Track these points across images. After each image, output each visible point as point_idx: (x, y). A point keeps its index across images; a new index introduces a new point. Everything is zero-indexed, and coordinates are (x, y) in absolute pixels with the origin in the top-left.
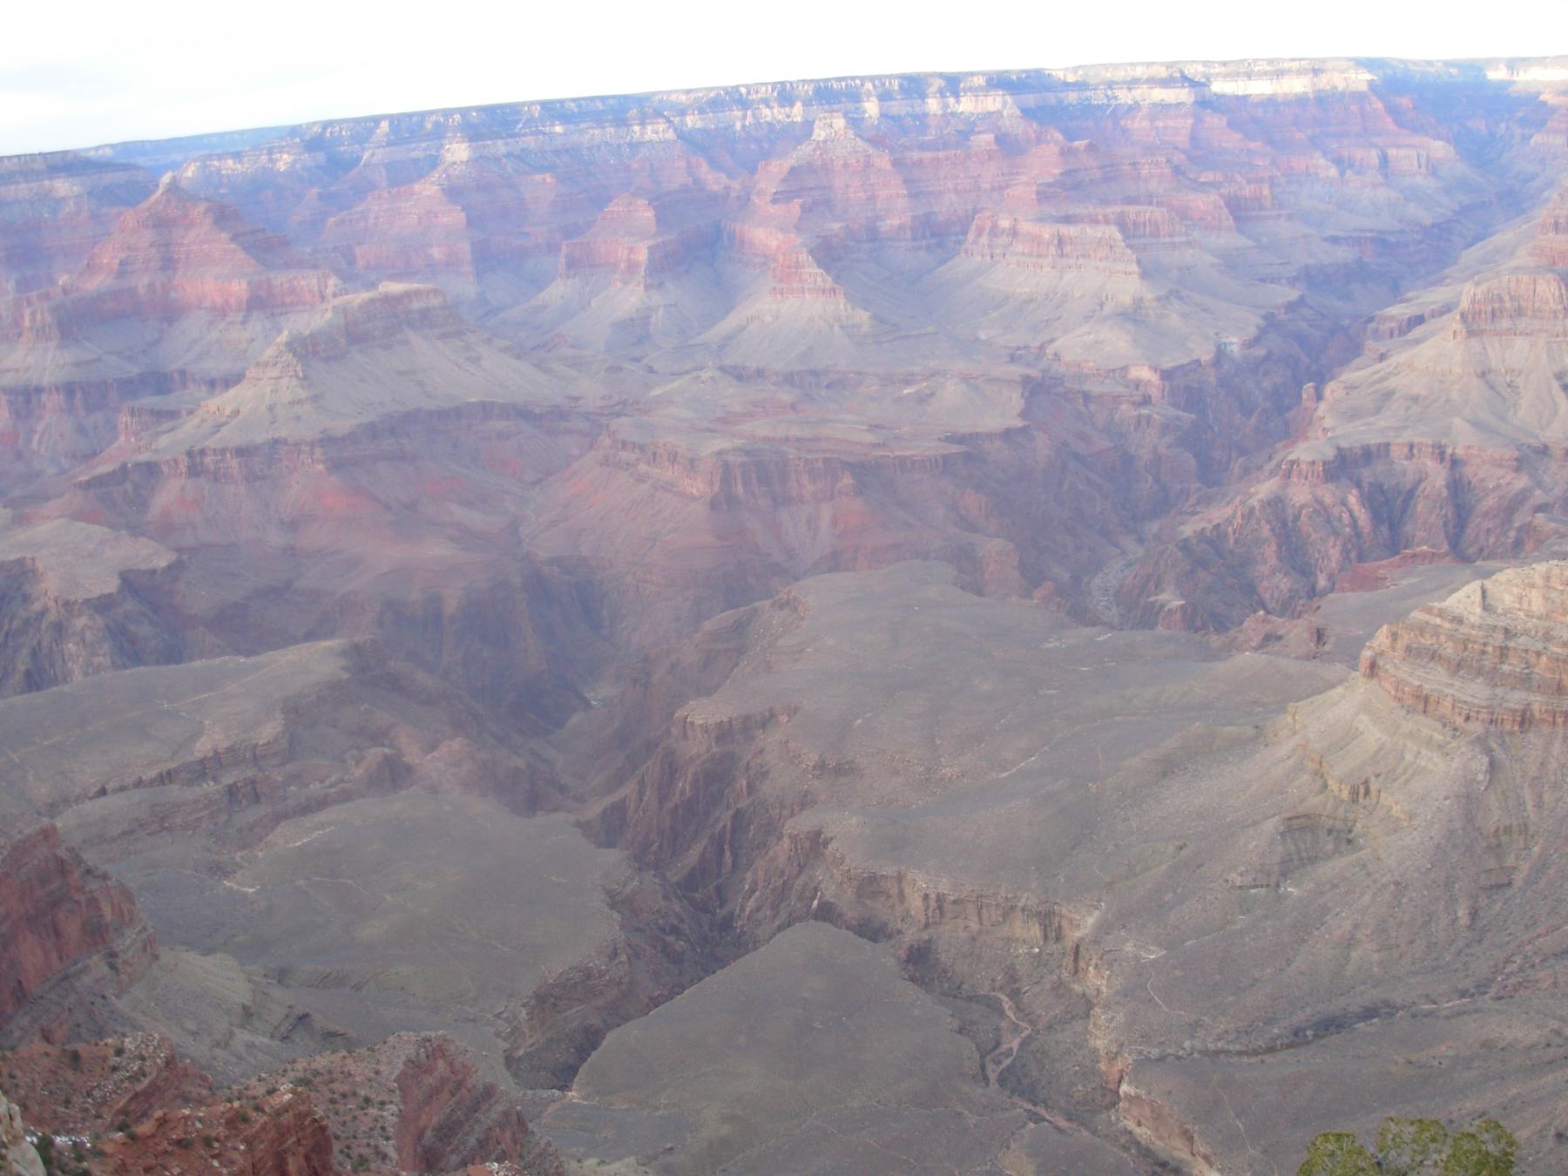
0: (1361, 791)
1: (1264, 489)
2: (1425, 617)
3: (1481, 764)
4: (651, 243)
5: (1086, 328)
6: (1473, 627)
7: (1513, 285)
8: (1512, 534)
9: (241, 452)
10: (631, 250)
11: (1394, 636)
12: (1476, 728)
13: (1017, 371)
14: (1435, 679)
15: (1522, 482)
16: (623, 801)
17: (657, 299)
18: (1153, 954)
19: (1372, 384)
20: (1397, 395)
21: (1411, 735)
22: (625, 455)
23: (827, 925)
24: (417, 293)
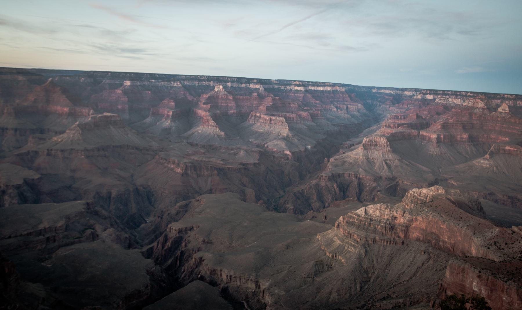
0: (334, 255)
1: (314, 182)
2: (351, 215)
3: (363, 251)
5: (275, 141)
6: (363, 218)
8: (372, 197)
9: (62, 151)
10: (168, 112)
11: (344, 219)
12: (363, 242)
13: (258, 149)
14: (353, 230)
15: (375, 184)
16: (153, 247)
17: (173, 124)
18: (283, 293)
21: (347, 243)
22: (162, 161)
23: (201, 282)
24: (114, 116)
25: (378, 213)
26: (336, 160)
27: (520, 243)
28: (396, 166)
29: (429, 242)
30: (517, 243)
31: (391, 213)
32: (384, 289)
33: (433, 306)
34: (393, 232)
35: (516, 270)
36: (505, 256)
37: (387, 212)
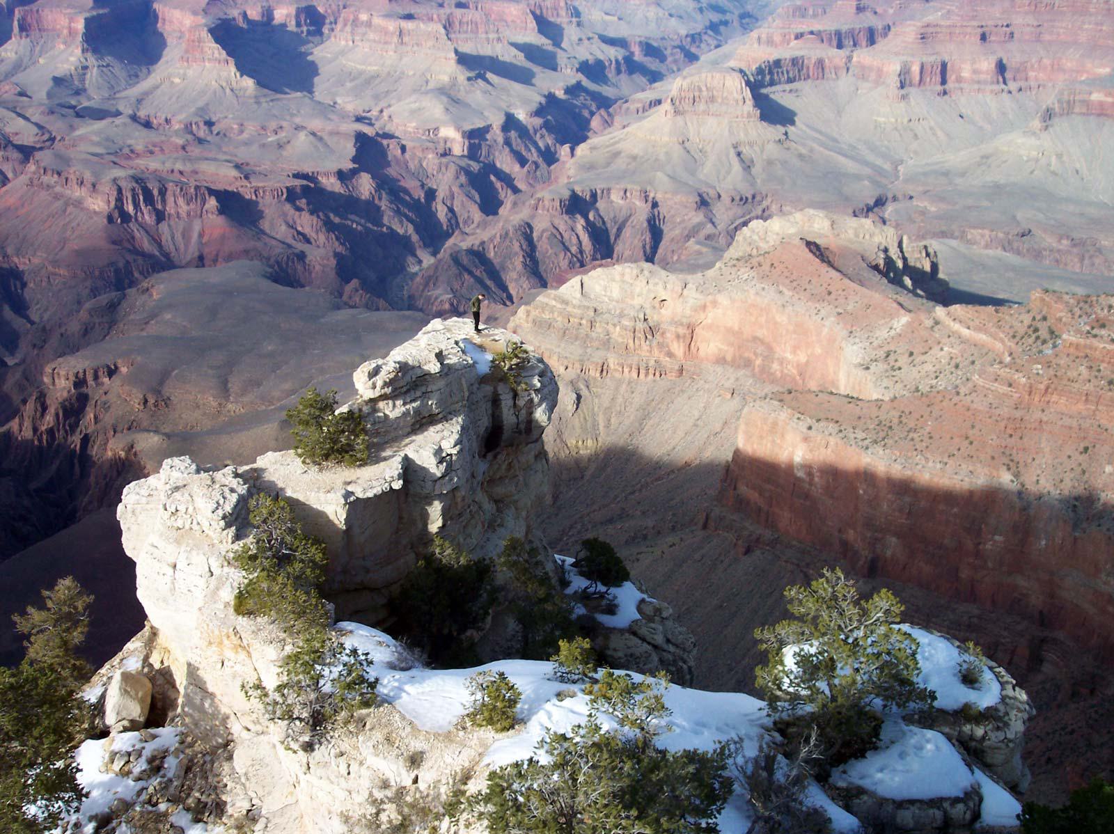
4: (88, 15)
6: (574, 307)
7: (709, 79)
10: (71, 20)
11: (528, 313)
17: (92, 60)
19: (608, 146)
20: (623, 155)
22: (47, 179)
25: (616, 292)
26: (593, 148)
27: (942, 349)
28: (770, 163)
29: (748, 364)
30: (936, 350)
31: (649, 291)
32: (616, 497)
33: (705, 527)
34: (655, 343)
35: (901, 416)
36: (899, 386)
37: (640, 286)
